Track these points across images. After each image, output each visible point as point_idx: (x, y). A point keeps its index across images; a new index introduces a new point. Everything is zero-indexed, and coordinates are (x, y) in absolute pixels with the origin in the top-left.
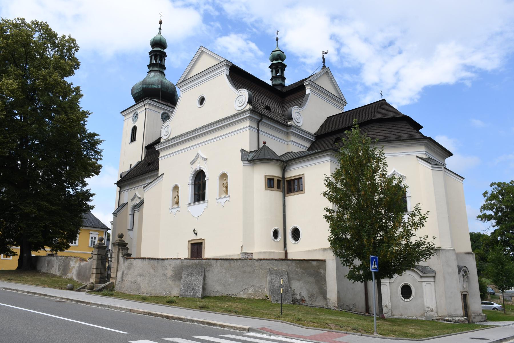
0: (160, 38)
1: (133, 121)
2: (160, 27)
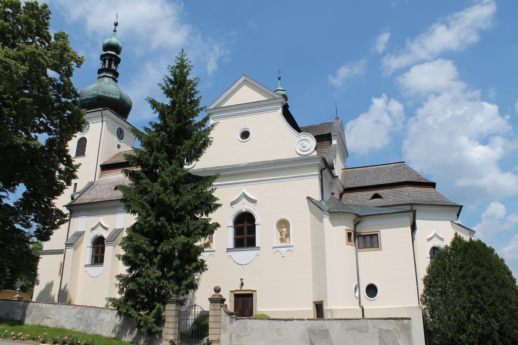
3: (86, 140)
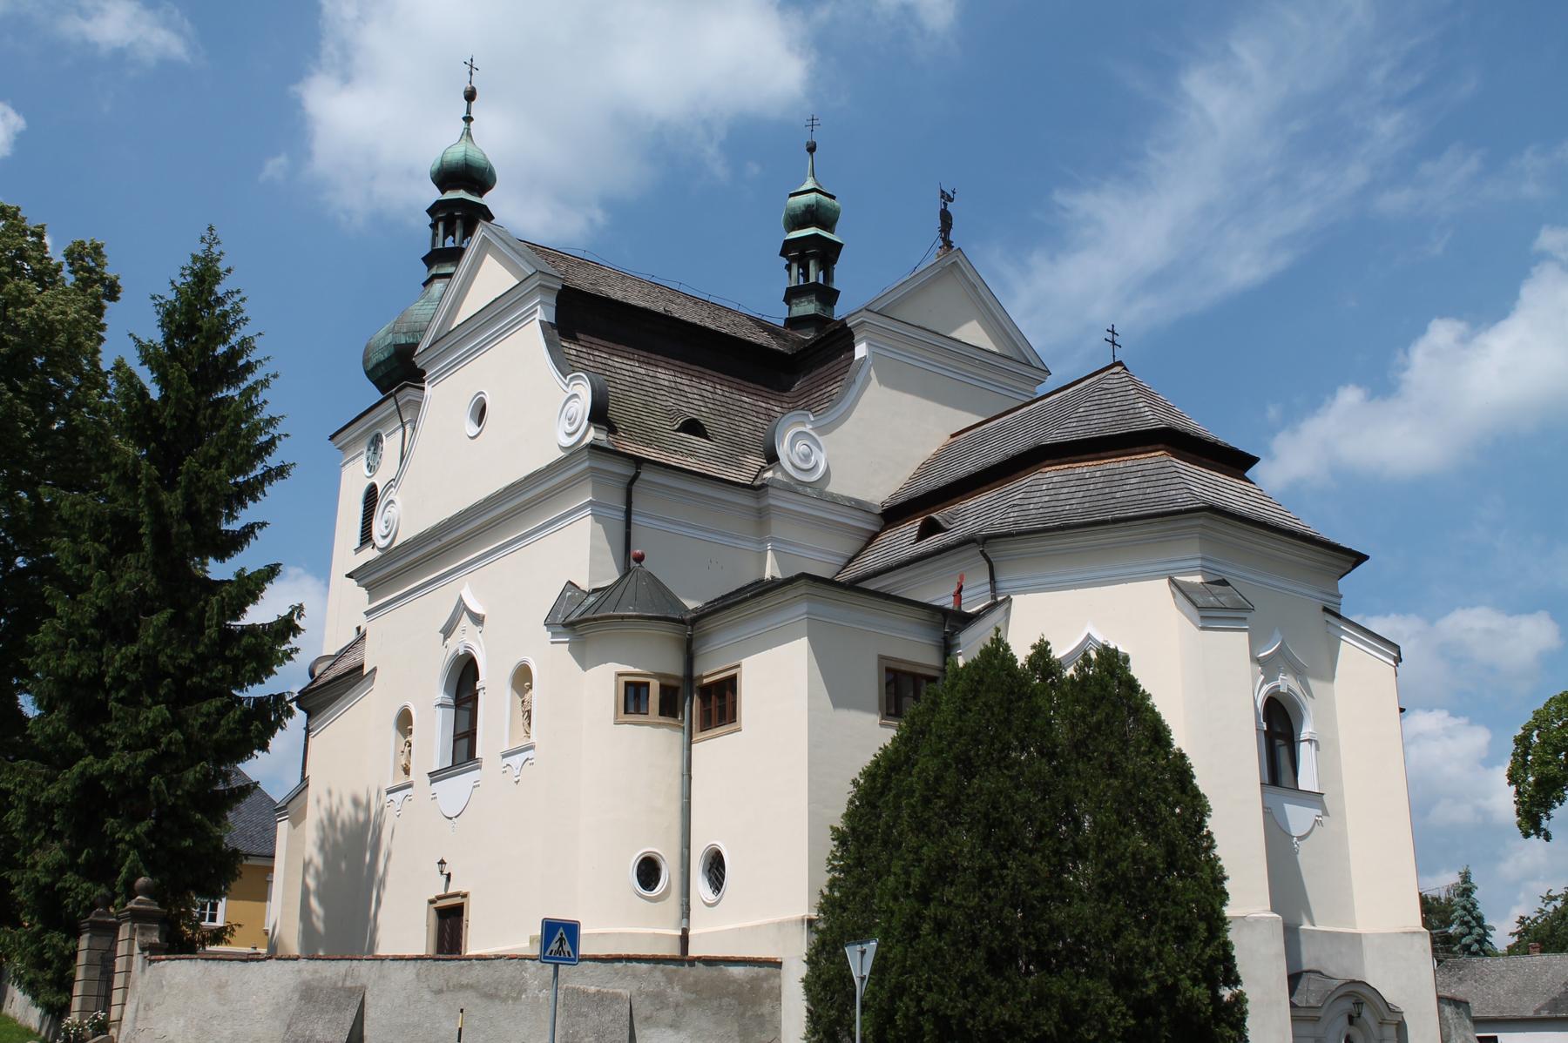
0: (465, 159)
2: (468, 112)
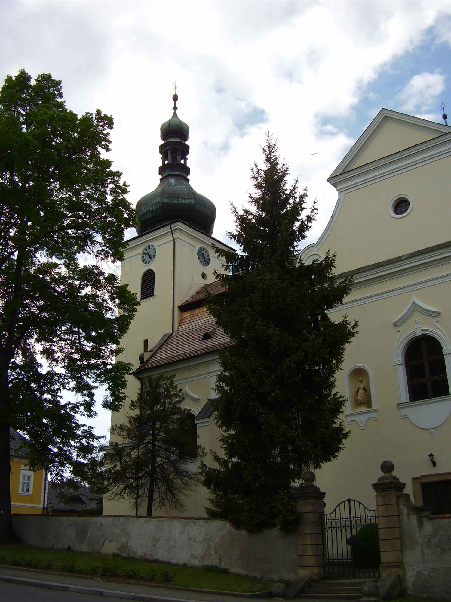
1: (143, 261)
3: (154, 273)
